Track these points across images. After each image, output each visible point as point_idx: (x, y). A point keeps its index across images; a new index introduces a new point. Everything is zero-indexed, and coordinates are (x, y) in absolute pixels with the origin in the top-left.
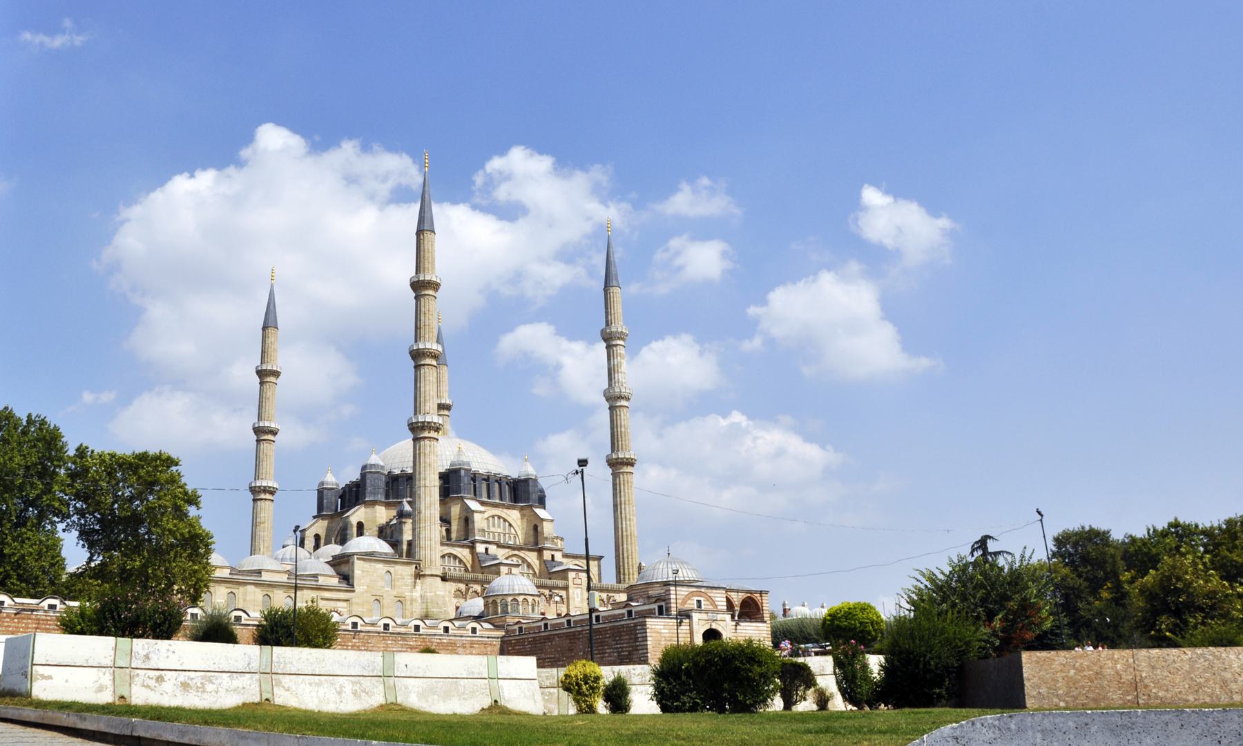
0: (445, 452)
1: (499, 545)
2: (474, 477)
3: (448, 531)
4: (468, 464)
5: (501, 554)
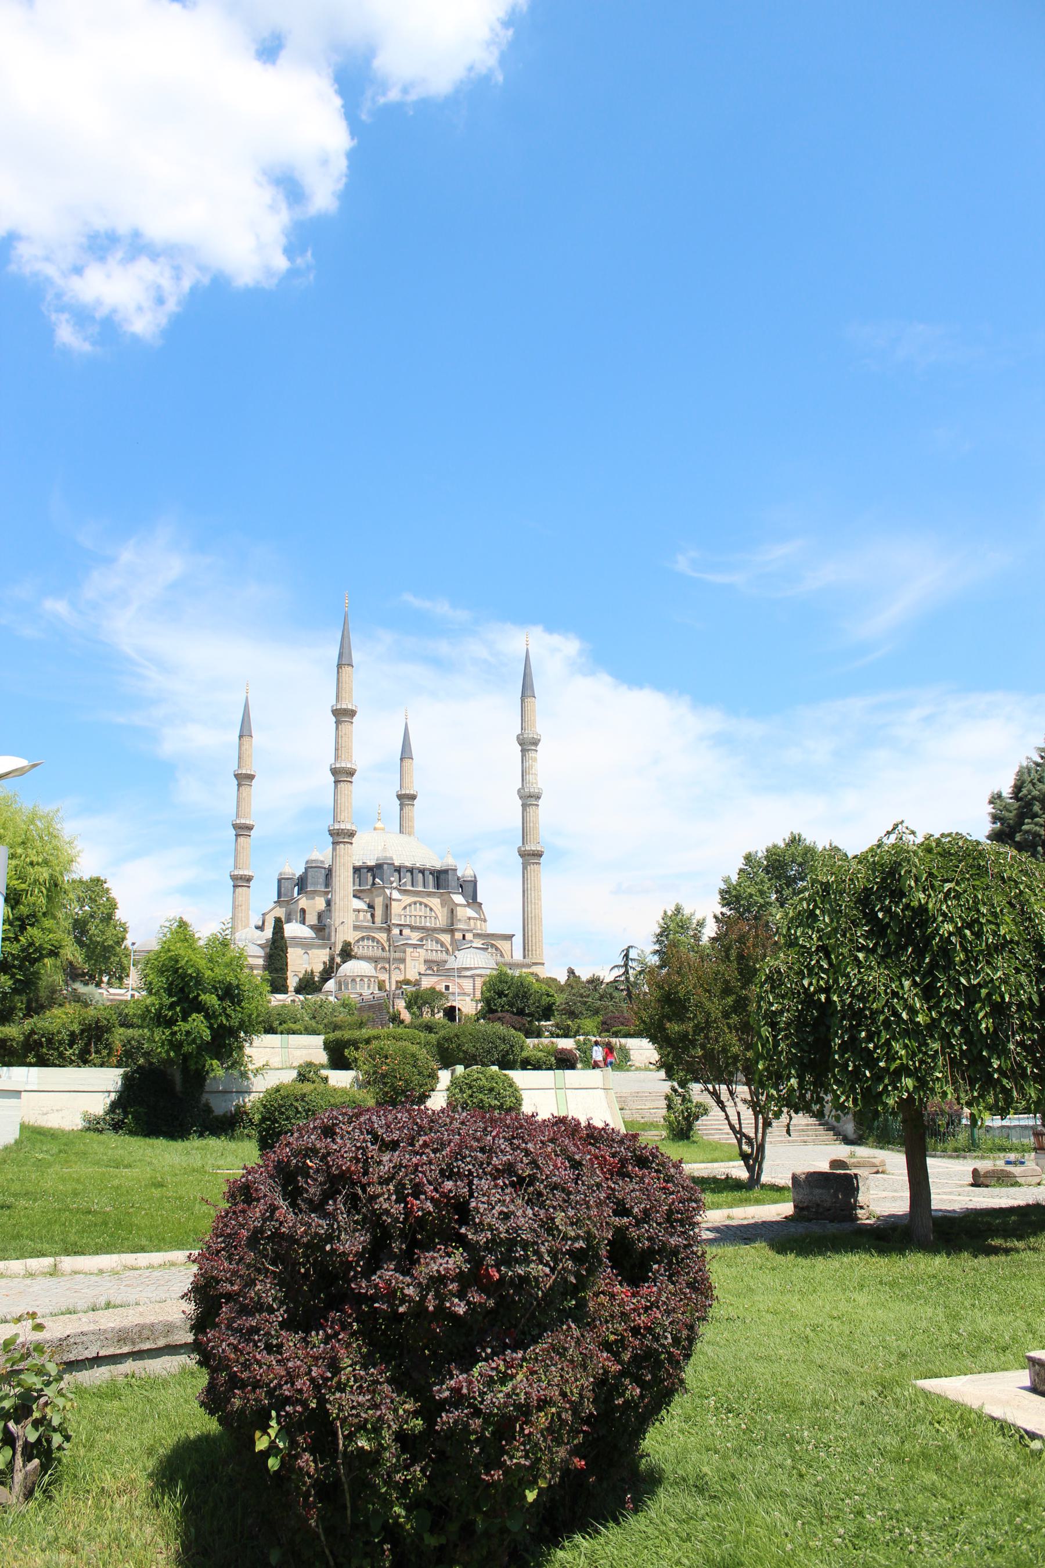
0: (366, 849)
1: (413, 928)
2: (398, 870)
3: (373, 916)
4: (391, 859)
5: (414, 937)
